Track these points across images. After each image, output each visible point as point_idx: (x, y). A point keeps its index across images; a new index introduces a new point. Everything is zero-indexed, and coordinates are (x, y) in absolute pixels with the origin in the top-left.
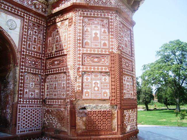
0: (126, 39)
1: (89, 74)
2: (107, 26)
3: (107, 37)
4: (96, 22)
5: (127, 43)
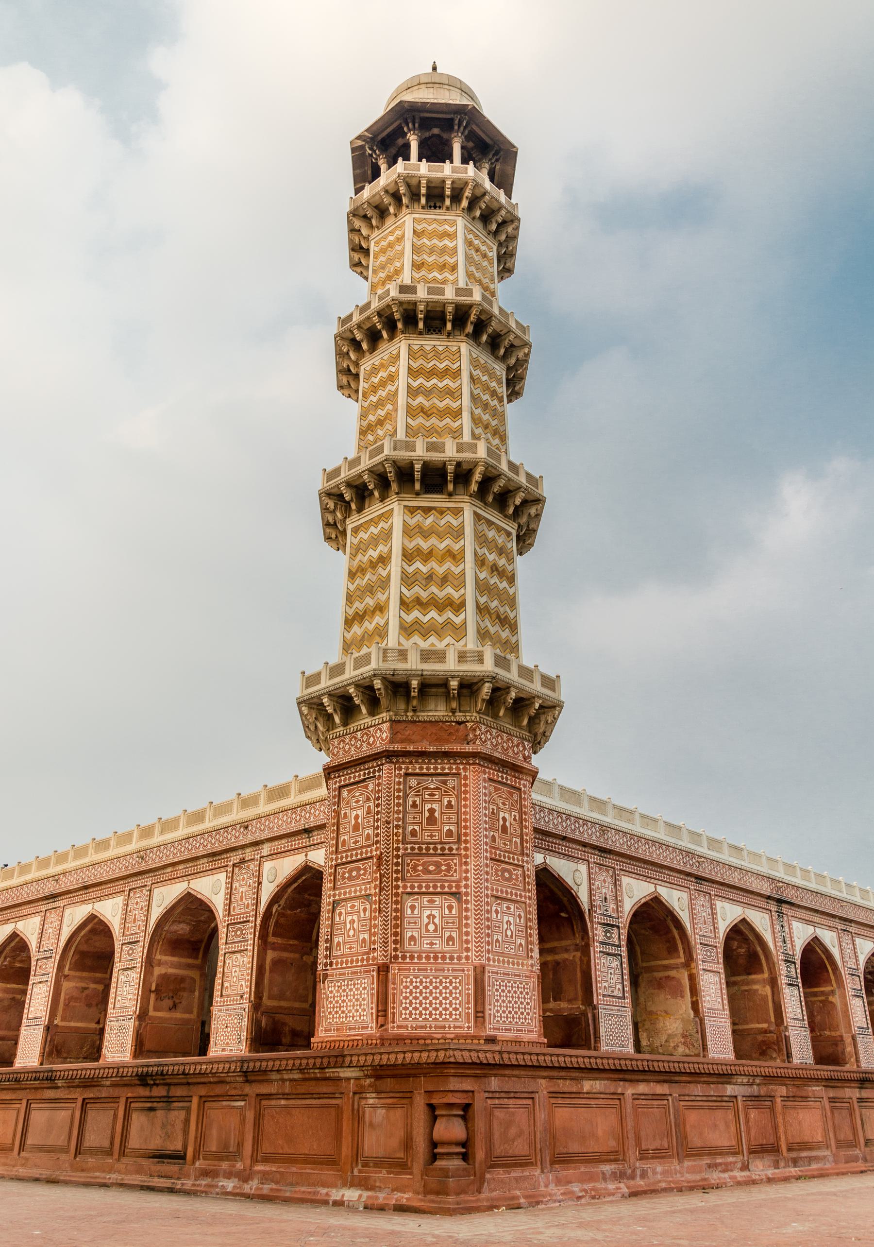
0: (507, 816)
4: (432, 787)
5: (507, 824)
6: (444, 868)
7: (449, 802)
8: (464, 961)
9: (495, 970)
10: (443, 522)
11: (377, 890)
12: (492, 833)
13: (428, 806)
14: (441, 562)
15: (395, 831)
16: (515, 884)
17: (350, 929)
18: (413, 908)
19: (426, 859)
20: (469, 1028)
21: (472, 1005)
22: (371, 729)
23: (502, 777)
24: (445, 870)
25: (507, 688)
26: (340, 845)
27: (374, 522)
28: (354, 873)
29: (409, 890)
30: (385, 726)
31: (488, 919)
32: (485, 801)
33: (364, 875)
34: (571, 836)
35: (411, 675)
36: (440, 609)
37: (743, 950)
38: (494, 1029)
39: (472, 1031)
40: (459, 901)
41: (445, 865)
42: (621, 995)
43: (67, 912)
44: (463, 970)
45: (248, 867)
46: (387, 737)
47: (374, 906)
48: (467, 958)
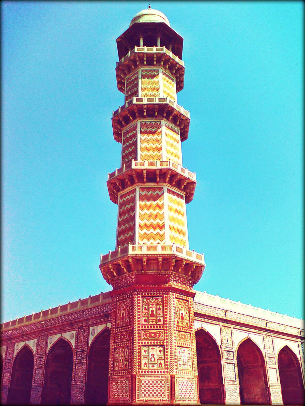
1: (146, 347)
2: (162, 304)
3: (162, 314)
4: (152, 301)
5: (183, 315)
6: (158, 335)
7: (159, 307)
8: (166, 373)
9: (179, 376)
10: (155, 193)
11: (131, 344)
12: (177, 320)
13: (151, 309)
14: (154, 209)
15: (138, 320)
16: (187, 340)
17: (121, 360)
18: (145, 351)
19: (150, 331)
20: (168, 400)
21: (169, 391)
22: (128, 278)
23: (181, 296)
24: (158, 336)
25: (182, 260)
26: (117, 325)
27: (128, 194)
28: (122, 337)
29: (144, 344)
30: (133, 277)
31: (176, 356)
32: (174, 307)
33: (126, 337)
34: (212, 315)
35: (143, 256)
36: (155, 228)
37: (287, 358)
38: (179, 401)
39: (169, 402)
40: (164, 348)
41: (158, 334)
42: (235, 380)
43: (16, 344)
44: (166, 377)
45: (84, 328)
46: (134, 281)
47: (130, 351)
48: (167, 372)
